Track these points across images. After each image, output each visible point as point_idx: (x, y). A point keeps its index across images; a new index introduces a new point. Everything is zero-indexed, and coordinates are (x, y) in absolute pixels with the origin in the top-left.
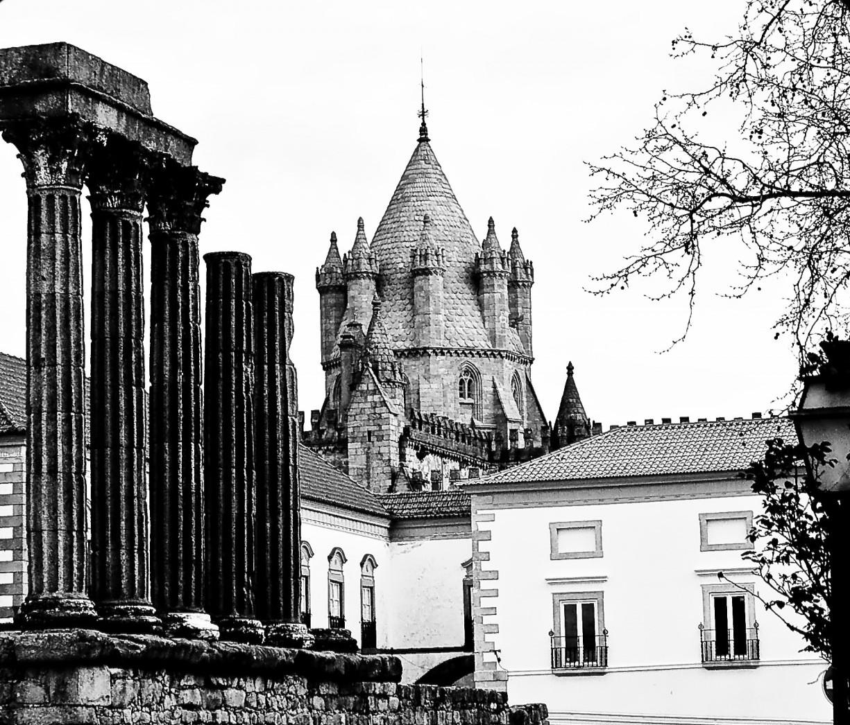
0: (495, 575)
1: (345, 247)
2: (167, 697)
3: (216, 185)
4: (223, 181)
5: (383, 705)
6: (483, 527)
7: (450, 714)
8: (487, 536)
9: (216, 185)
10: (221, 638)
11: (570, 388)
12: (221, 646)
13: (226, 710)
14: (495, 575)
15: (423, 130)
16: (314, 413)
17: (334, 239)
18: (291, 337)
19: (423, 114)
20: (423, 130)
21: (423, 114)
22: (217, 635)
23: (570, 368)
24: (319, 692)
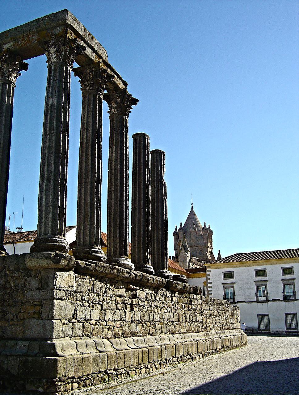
0: (211, 283)
1: (178, 228)
2: (108, 290)
3: (135, 102)
4: (138, 101)
5: (196, 302)
6: (208, 273)
7: (216, 307)
8: (209, 275)
9: (135, 102)
10: (134, 270)
11: (219, 253)
12: (135, 272)
13: (137, 299)
14: (211, 283)
15: (192, 207)
16: (173, 257)
17: (176, 227)
18: (164, 171)
19: (192, 204)
20: (192, 207)
21: (192, 204)
22: (133, 267)
23: (219, 251)
24: (175, 295)
